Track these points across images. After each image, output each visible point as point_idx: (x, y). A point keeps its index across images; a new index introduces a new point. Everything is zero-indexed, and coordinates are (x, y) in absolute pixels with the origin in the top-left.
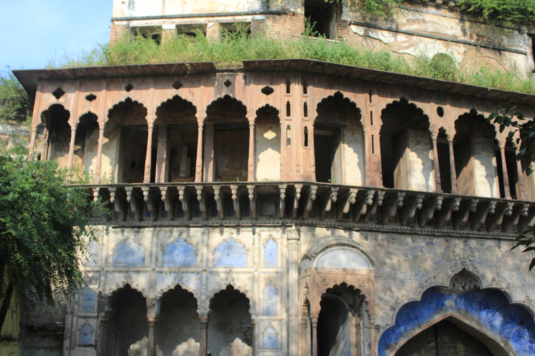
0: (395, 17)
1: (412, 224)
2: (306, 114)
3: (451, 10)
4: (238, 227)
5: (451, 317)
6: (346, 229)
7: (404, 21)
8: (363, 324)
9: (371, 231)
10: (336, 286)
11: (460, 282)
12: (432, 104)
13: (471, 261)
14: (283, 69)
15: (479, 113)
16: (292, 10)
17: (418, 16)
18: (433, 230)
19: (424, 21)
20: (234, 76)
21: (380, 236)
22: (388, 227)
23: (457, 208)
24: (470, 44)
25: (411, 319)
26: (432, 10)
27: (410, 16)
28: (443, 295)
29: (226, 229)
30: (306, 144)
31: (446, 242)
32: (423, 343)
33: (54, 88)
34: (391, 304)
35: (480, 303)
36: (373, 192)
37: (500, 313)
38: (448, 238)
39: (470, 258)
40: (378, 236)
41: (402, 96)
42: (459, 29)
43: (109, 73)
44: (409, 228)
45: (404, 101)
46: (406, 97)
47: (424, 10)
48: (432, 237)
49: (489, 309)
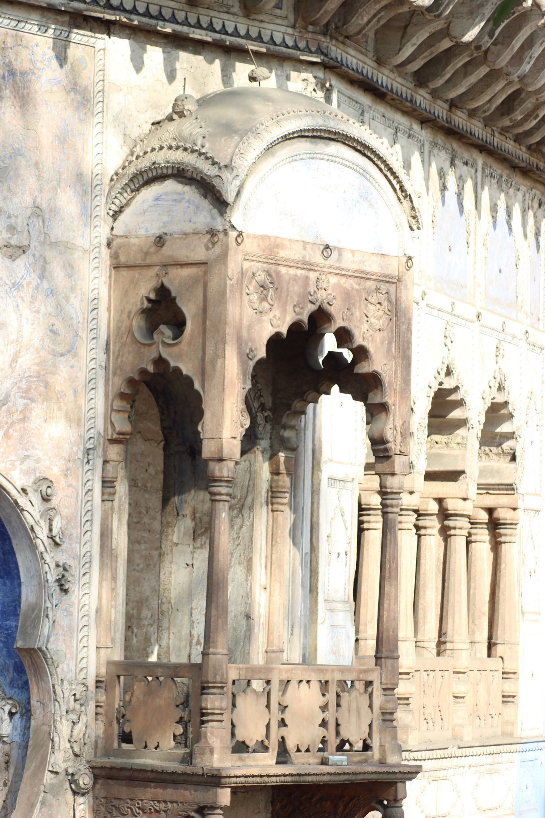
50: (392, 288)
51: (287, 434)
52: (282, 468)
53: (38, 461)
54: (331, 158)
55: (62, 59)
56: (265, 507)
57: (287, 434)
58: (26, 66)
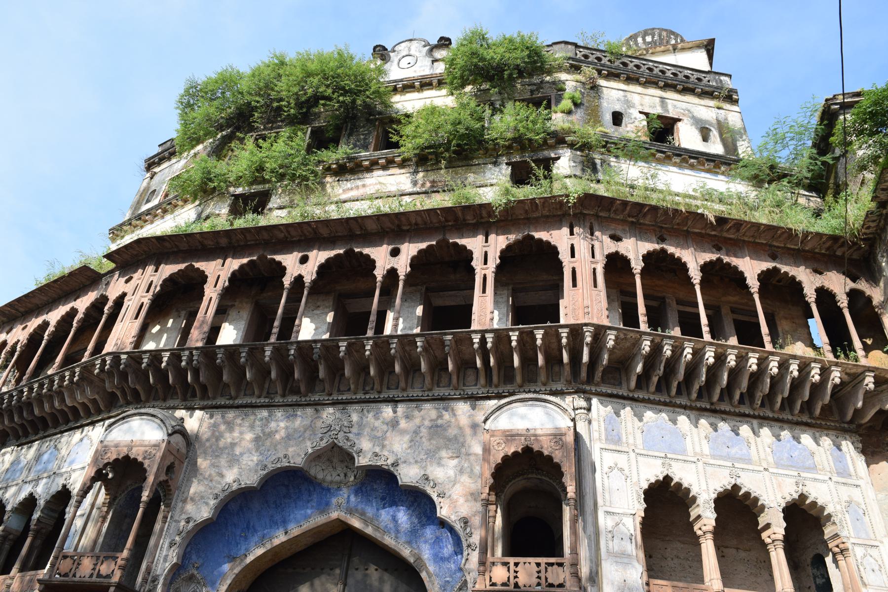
0: (329, 190)
2: (148, 291)
3: (403, 164)
4: (93, 423)
5: (338, 520)
7: (341, 191)
8: (172, 517)
10: (116, 460)
12: (295, 253)
15: (357, 250)
16: (217, 212)
17: (359, 183)
18: (299, 399)
19: (364, 186)
20: (113, 276)
23: (291, 357)
24: (418, 193)
25: (276, 523)
26: (381, 172)
27: (349, 185)
28: (329, 490)
29: (86, 428)
30: (136, 318)
32: (322, 569)
33: (7, 328)
34: (216, 492)
35: (383, 499)
36: (187, 353)
38: (319, 407)
39: (346, 430)
41: (261, 252)
42: (409, 181)
43: (36, 301)
44: (267, 400)
45: (262, 258)
47: (368, 175)
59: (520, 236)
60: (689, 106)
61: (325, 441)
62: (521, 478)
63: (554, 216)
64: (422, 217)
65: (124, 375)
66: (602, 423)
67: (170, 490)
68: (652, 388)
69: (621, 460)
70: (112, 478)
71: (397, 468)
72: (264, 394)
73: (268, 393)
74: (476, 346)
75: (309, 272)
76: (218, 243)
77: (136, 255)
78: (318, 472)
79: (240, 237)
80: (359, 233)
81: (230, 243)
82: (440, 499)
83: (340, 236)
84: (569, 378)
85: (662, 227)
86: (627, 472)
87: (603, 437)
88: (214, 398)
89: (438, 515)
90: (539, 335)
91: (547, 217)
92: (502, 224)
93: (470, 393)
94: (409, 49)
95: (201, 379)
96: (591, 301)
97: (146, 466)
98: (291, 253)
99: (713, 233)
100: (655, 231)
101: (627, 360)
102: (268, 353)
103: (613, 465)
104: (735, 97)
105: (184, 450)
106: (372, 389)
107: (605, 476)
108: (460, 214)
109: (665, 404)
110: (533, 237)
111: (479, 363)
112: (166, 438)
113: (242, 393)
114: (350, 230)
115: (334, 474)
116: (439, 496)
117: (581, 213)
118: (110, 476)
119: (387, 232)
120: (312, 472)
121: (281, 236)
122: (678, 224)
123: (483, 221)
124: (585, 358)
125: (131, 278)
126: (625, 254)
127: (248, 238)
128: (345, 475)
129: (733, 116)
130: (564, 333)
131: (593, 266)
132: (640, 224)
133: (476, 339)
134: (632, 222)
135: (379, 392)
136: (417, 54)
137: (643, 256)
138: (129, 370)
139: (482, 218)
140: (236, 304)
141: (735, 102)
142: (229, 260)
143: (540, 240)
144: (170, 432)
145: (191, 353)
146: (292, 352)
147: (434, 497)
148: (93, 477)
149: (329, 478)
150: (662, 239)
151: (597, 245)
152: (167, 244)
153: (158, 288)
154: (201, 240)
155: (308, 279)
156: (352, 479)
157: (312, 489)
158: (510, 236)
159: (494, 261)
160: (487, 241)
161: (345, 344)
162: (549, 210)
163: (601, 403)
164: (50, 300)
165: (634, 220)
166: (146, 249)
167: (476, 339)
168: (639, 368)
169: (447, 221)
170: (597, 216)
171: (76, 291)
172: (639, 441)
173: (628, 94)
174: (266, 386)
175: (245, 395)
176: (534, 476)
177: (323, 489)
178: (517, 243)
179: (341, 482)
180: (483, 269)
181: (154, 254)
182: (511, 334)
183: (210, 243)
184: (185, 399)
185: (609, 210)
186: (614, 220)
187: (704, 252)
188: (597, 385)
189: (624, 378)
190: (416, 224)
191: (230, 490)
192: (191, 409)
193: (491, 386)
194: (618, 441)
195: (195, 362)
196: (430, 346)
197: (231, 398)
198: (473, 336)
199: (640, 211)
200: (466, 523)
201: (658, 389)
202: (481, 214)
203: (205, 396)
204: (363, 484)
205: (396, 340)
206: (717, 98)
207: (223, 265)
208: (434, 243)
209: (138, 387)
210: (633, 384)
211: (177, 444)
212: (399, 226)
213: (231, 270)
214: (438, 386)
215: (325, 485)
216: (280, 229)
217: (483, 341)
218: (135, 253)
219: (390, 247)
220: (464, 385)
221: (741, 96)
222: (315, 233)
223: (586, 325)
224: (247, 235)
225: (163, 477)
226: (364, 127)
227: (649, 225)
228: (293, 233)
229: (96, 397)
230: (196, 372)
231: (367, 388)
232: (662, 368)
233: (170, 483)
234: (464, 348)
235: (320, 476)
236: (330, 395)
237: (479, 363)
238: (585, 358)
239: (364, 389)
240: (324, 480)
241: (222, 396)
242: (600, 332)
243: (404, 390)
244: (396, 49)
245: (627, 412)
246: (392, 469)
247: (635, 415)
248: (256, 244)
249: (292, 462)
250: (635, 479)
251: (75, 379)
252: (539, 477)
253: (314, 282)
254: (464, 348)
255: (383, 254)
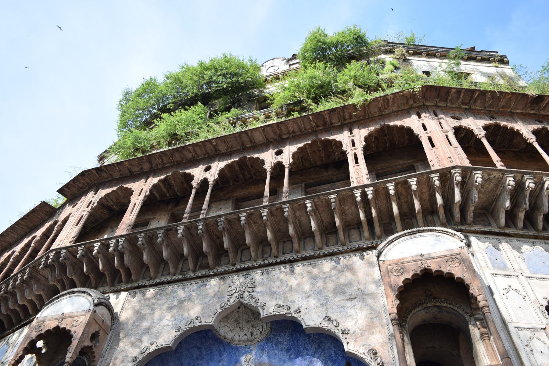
1: (185, 273)
2: (88, 207)
6: (114, 292)
9: (138, 287)
11: (258, 328)
13: (249, 292)
14: (87, 188)
21: (151, 292)
22: (158, 281)
23: (200, 231)
28: (237, 349)
30: (77, 225)
31: (222, 280)
35: (288, 350)
36: (114, 241)
37: (318, 358)
38: (225, 276)
39: (251, 290)
40: (146, 292)
41: (175, 170)
46: (178, 170)
48: (205, 279)
49: (302, 356)
50: (459, 257)
51: (477, 316)
52: (479, 326)
53: (370, 345)
54: (417, 237)
55: (362, 259)
56: (481, 341)
57: (477, 316)
58: (351, 263)
59: (378, 126)
60: (476, 67)
61: (232, 301)
62: (420, 308)
63: (402, 110)
64: (298, 125)
65: (63, 268)
66: (485, 255)
67: (94, 357)
68: (520, 224)
69: (514, 283)
70: (45, 353)
71: (299, 314)
72: (179, 272)
73: (181, 271)
74: (358, 199)
75: (212, 175)
76: (142, 169)
77: (81, 188)
78: (226, 332)
79: (159, 160)
80: (250, 146)
81: (151, 168)
82: (345, 336)
83: (235, 151)
84: (444, 220)
85: (490, 111)
86: (522, 292)
87: (490, 265)
88: (137, 281)
89: (346, 349)
90: (413, 182)
91: (397, 111)
92: (361, 122)
93: (356, 247)
94: (273, 63)
95: (125, 262)
96: (452, 153)
97: (72, 333)
98: (198, 166)
99: (532, 112)
100: (485, 113)
101: (491, 204)
102: (180, 231)
103: (507, 287)
104: (505, 60)
105: (109, 323)
106: (270, 256)
107: (504, 297)
108: (327, 117)
109: (536, 238)
110: (389, 126)
111: (362, 215)
112: (92, 308)
113: (160, 274)
114: (243, 144)
115: (242, 334)
116: (343, 332)
117: (424, 105)
118: (44, 351)
119: (271, 142)
120: (222, 332)
121: (190, 156)
122: (503, 107)
123: (346, 122)
124: (458, 197)
125: (77, 204)
126: (468, 126)
127: (165, 161)
128: (252, 334)
129: (508, 71)
130: (436, 180)
131: (445, 134)
132: (473, 109)
133: (358, 194)
134: (466, 109)
135: (276, 257)
136: (279, 65)
137: (482, 127)
138: (66, 262)
139: (345, 120)
140: (157, 217)
141: (507, 63)
142: (150, 179)
143: (396, 126)
144: (96, 302)
145: (118, 241)
146: (201, 227)
147: (340, 335)
148: (26, 348)
149: (237, 338)
150: (492, 118)
151: (442, 121)
152: (104, 174)
153: (96, 204)
154: (129, 167)
155: (211, 180)
156: (259, 335)
157: (222, 349)
158: (370, 128)
159: (360, 145)
160: (351, 133)
161: (245, 214)
162: (398, 106)
163: (479, 239)
164: (19, 238)
165: (467, 107)
166: (89, 181)
167: (358, 194)
168: (508, 204)
169: (317, 126)
170: (437, 106)
171: (38, 226)
172: (524, 266)
173: (431, 63)
174: (180, 266)
175: (162, 275)
176: (433, 304)
177: (232, 348)
178: (376, 131)
179: (248, 340)
180: (352, 150)
181: (95, 184)
182: (388, 185)
183: (136, 169)
184: (112, 285)
185: (446, 100)
186: (450, 108)
187: (530, 124)
188: (469, 225)
189: (492, 221)
190: (294, 132)
191: (148, 352)
192: (117, 292)
193: (374, 239)
194: (505, 267)
195: (120, 247)
196: (317, 209)
197: (151, 279)
198: (355, 192)
199: (472, 98)
200: (375, 354)
201: (525, 227)
202: (344, 116)
203: (129, 279)
204: (268, 339)
205: (287, 205)
206: (494, 61)
207: (146, 182)
208: (310, 142)
209: (74, 278)
210: (503, 221)
211: (102, 315)
212: (280, 136)
213: (152, 184)
214: (327, 245)
215: (234, 344)
216: (188, 149)
217: (364, 195)
218: (80, 185)
219: (275, 151)
220: (350, 241)
221: (510, 58)
222: (216, 150)
223: (454, 168)
224: (164, 158)
225: (87, 343)
226: (246, 104)
227: (479, 110)
228: (199, 152)
229: (41, 293)
230: (121, 256)
231: (265, 256)
232: (527, 202)
233: (94, 349)
234: (346, 208)
235: (229, 336)
236: (234, 265)
237: (362, 215)
238: (458, 197)
239: (263, 257)
240: (232, 340)
241: (143, 278)
242: (466, 172)
243: (298, 252)
244: (264, 65)
245: (505, 246)
246: (295, 316)
247: (513, 248)
248: (171, 166)
249: (203, 321)
250: (533, 298)
251: (25, 277)
252: (438, 304)
253: (216, 181)
254: (346, 208)
255: (270, 155)
